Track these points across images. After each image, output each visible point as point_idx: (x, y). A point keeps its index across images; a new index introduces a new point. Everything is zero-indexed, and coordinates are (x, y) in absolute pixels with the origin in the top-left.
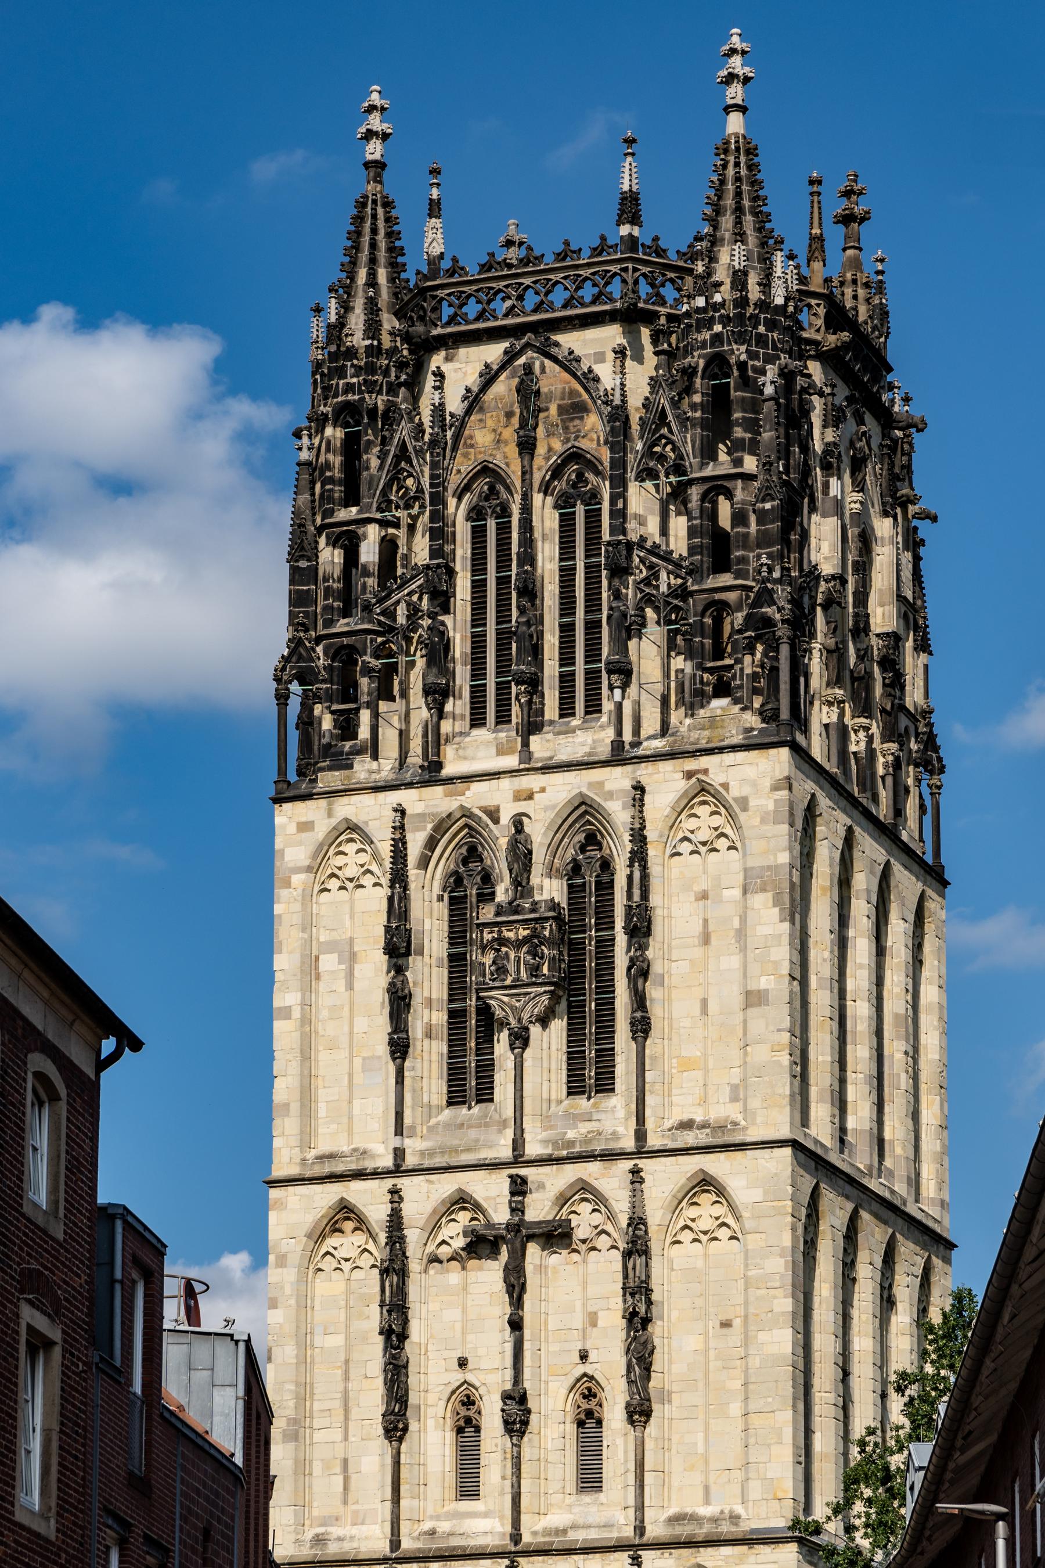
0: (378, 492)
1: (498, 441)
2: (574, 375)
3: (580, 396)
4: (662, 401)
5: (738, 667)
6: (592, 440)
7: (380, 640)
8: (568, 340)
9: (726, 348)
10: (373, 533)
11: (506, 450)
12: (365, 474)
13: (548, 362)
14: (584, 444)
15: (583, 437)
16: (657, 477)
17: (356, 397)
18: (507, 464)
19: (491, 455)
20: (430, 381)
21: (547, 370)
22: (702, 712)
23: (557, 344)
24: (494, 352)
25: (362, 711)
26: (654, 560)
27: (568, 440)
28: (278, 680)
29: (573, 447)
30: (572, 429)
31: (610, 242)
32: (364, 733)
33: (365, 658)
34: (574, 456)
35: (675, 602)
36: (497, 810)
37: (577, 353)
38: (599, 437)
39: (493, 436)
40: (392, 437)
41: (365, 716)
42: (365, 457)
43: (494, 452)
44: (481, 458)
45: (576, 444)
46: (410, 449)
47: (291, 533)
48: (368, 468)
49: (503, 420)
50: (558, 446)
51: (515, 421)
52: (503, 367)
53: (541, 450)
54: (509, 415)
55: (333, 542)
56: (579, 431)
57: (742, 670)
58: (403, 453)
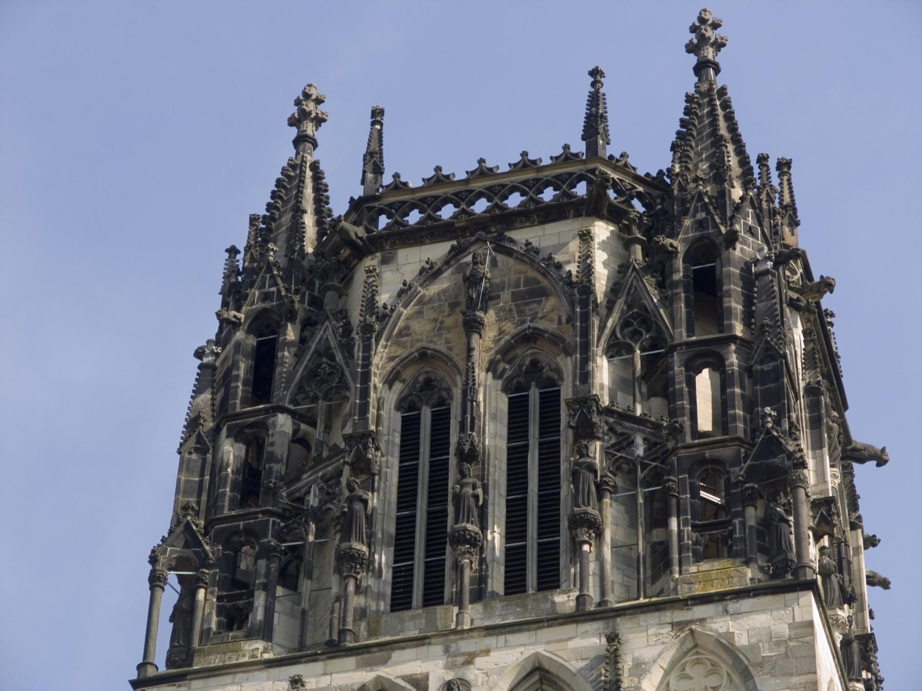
0: (293, 385)
1: (439, 329)
2: (532, 263)
3: (538, 282)
4: (635, 283)
5: (736, 521)
6: (551, 320)
7: (282, 524)
8: (521, 236)
9: (711, 231)
10: (283, 423)
11: (449, 336)
12: (278, 370)
13: (500, 258)
14: (542, 325)
15: (541, 318)
16: (631, 351)
17: (274, 303)
18: (450, 349)
19: (431, 342)
20: (360, 276)
21: (500, 264)
22: (693, 569)
23: (511, 240)
24: (438, 251)
25: (256, 593)
26: (627, 424)
27: (523, 322)
28: (153, 560)
29: (529, 328)
30: (528, 312)
31: (573, 150)
32: (259, 614)
33: (265, 540)
34: (528, 338)
35: (654, 464)
36: (426, 677)
37: (535, 244)
38: (560, 318)
39: (433, 325)
40: (313, 334)
41: (260, 600)
42: (280, 354)
43: (435, 339)
44: (419, 345)
45: (533, 325)
46: (333, 343)
47: (185, 427)
48: (283, 363)
49: (447, 309)
50: (510, 328)
51: (463, 307)
52: (447, 262)
53: (490, 333)
54: (453, 306)
55: (237, 435)
56: (537, 313)
57: (743, 524)
58: (325, 352)
